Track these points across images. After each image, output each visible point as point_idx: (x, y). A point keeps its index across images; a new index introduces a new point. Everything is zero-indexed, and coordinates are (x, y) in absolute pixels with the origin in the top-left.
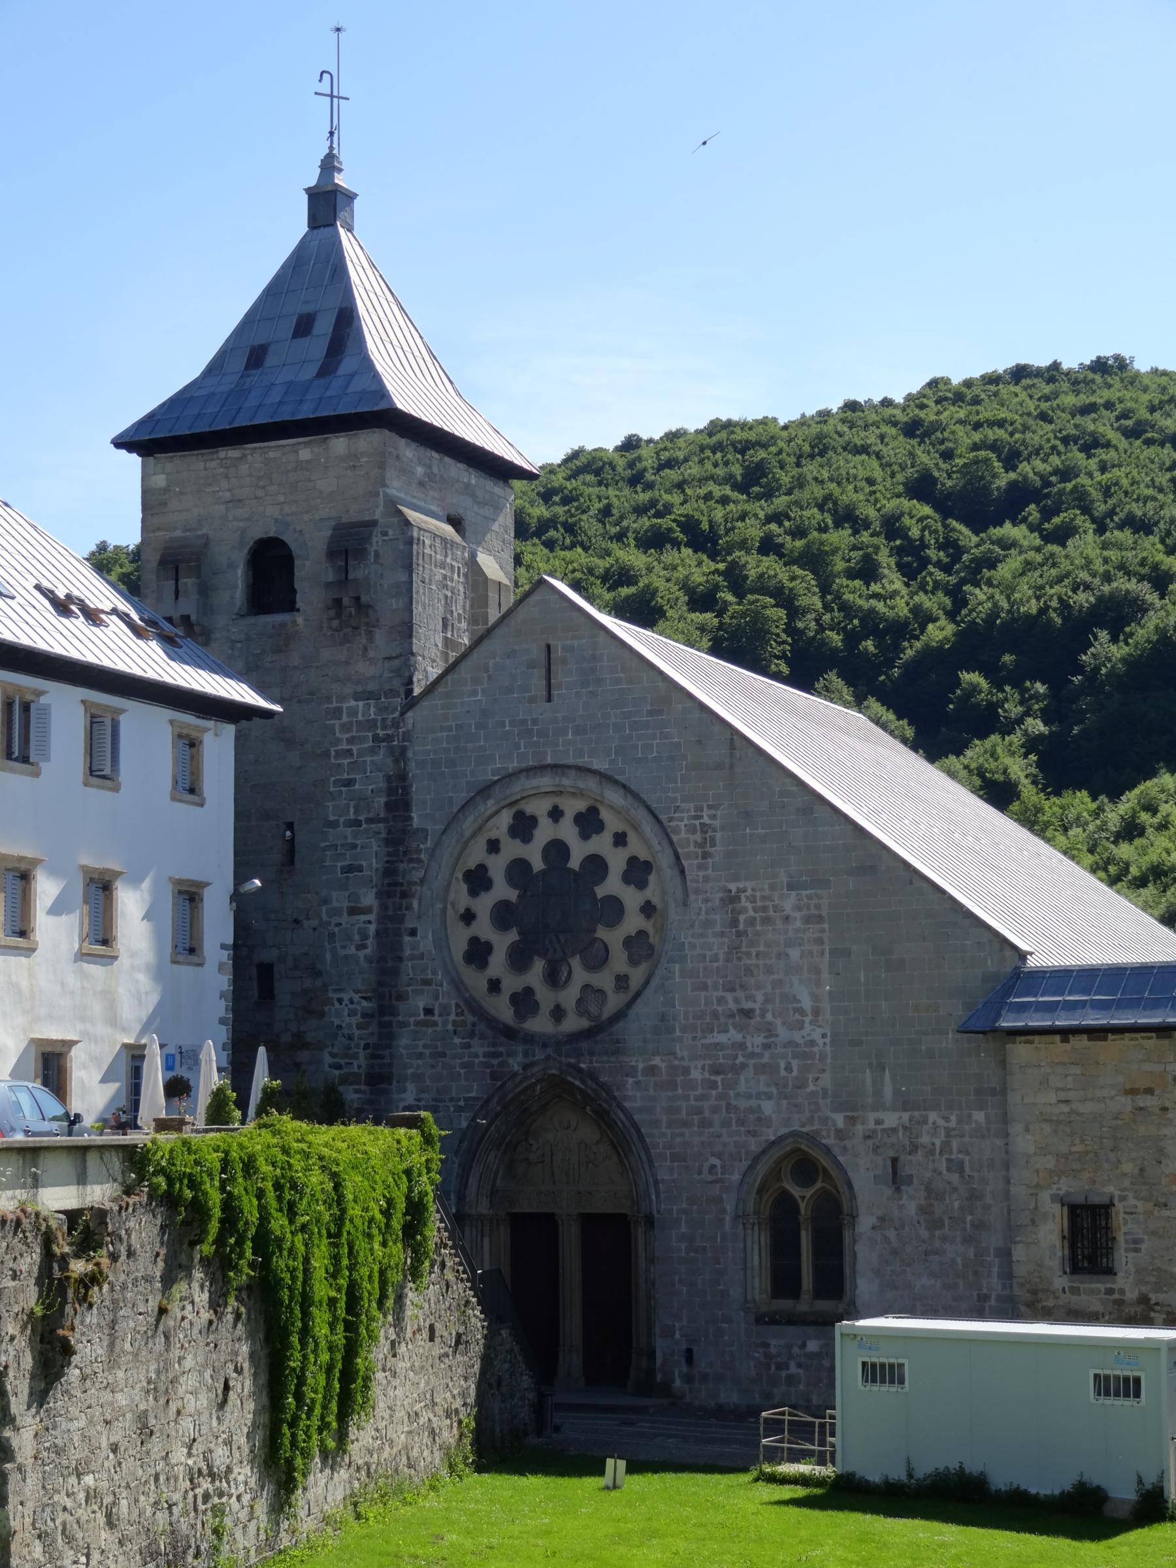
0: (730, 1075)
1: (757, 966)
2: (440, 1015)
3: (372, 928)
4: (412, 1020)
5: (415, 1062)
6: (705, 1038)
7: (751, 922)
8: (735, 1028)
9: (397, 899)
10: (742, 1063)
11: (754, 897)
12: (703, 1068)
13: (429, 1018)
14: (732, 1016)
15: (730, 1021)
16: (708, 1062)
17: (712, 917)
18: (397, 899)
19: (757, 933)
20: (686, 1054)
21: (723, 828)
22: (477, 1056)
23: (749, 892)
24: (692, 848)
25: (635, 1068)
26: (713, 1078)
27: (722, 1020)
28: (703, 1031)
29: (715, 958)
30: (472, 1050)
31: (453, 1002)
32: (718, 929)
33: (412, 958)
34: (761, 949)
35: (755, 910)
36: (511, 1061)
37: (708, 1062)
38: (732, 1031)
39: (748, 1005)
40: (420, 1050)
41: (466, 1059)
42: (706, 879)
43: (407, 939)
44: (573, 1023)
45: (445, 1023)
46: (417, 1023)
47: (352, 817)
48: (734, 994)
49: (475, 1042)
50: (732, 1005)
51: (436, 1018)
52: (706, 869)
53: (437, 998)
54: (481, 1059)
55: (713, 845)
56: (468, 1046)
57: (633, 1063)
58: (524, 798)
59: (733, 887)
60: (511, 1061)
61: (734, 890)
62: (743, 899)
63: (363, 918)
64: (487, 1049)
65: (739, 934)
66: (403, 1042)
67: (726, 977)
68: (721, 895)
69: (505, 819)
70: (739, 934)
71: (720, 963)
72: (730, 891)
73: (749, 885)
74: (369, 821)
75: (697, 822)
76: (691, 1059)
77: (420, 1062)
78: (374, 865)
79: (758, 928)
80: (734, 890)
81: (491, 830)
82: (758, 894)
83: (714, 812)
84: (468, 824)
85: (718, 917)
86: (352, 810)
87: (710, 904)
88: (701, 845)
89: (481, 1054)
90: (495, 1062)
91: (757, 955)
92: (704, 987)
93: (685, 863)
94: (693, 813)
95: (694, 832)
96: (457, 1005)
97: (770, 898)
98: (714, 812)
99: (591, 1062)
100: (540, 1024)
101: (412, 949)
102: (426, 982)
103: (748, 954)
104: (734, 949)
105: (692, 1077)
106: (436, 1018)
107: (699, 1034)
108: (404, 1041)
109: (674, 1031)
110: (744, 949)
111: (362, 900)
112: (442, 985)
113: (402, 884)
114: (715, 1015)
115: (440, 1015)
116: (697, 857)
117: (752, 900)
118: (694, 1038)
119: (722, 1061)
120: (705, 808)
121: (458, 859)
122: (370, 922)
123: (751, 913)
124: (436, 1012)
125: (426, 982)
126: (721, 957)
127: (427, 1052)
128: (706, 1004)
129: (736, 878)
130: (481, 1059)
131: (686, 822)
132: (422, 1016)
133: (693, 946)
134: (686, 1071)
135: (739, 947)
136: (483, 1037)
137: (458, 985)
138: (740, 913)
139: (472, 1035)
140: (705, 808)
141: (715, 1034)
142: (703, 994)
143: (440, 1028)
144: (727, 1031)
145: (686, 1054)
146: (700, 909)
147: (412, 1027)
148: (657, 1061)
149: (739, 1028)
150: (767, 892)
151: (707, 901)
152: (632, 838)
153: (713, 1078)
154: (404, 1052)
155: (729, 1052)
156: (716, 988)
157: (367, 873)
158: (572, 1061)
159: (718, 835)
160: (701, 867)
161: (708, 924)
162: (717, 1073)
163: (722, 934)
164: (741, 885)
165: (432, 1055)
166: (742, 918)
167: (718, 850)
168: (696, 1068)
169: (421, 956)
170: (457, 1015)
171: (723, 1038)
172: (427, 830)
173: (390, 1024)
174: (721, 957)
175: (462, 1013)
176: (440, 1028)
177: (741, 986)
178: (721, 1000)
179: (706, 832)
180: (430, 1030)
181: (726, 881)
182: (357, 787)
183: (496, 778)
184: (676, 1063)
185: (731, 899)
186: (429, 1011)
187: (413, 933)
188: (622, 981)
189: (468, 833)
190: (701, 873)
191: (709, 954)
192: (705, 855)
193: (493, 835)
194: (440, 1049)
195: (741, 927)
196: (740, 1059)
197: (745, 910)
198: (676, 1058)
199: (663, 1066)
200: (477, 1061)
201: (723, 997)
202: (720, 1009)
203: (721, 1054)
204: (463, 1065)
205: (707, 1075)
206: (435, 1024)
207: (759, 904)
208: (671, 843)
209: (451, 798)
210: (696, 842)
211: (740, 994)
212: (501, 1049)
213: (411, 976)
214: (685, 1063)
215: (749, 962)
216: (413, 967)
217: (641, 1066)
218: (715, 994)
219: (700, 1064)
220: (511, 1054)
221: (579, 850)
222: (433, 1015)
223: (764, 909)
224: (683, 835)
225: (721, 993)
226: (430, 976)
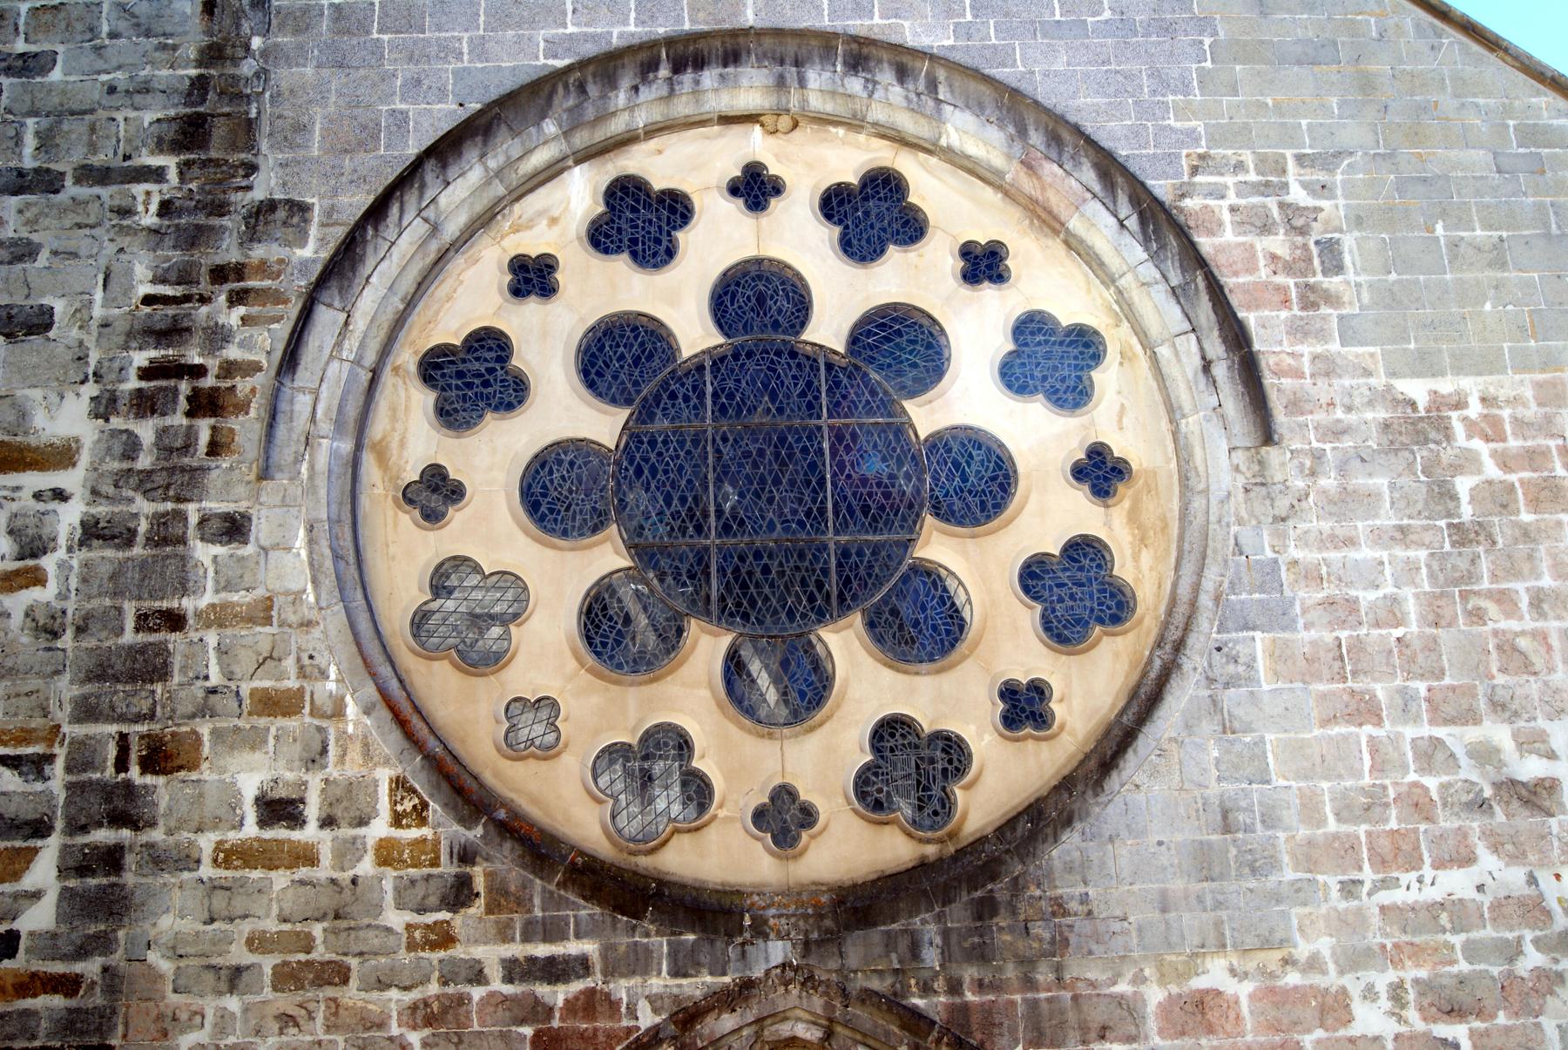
0: (1502, 1019)
1: (1541, 637)
2: (328, 822)
3: (69, 517)
4: (206, 843)
5: (210, 1005)
6: (1386, 884)
7: (1499, 498)
8: (1496, 849)
9: (178, 419)
10: (1539, 973)
11: (1496, 423)
12: (1397, 993)
13: (280, 833)
14: (1482, 805)
15: (1475, 825)
16: (1413, 972)
17: (1360, 481)
18: (178, 419)
19: (1526, 533)
20: (1324, 945)
21: (1358, 222)
22: (479, 977)
23: (1475, 410)
24: (1264, 273)
25: (1130, 1008)
26: (1444, 1030)
27: (1447, 822)
28: (1380, 862)
29: (1392, 613)
30: (459, 952)
31: (384, 776)
32: (1387, 519)
33: (218, 617)
34: (1547, 582)
35: (1505, 463)
36: (621, 988)
37: (1413, 972)
38: (1488, 861)
39: (1531, 769)
40: (239, 954)
41: (433, 988)
42: (1327, 367)
43: (204, 553)
44: (850, 847)
45: (348, 852)
46: (228, 856)
47: (29, 163)
48: (1472, 734)
49: (462, 921)
50: (1468, 771)
51: (310, 832)
52: (1322, 335)
53: (316, 757)
54: (497, 985)
55: (1334, 265)
56: (443, 938)
57: (1123, 987)
58: (652, 131)
59: (1417, 390)
60: (621, 988)
61: (1422, 402)
62: (1459, 429)
63: (33, 480)
64: (517, 950)
65: (1462, 536)
66: (171, 917)
67: (1441, 674)
68: (1382, 414)
69: (580, 194)
70: (1462, 536)
71: (1413, 627)
72: (1413, 405)
73: (1471, 385)
74: (92, 175)
75: (1272, 203)
76: (1354, 960)
77: (233, 1003)
78: (98, 312)
79: (1526, 517)
80: (1422, 402)
81: (530, 225)
82: (1506, 413)
83: (1322, 177)
84: (460, 192)
85: (1381, 482)
86: (30, 142)
87: (1348, 443)
88: (1297, 265)
89: (495, 973)
90: (559, 995)
91: (1538, 601)
92: (1367, 710)
93: (1250, 318)
94: (1252, 177)
95: (1266, 228)
96: (399, 784)
97: (1547, 426)
98: (1322, 177)
99: (954, 987)
100: (721, 854)
101: (226, 586)
102: (275, 704)
103: (1505, 600)
104: (1453, 590)
105: (1355, 1030)
106: (310, 832)
107: (1368, 875)
108: (167, 924)
109: (1274, 864)
110: (1485, 584)
111: (39, 420)
112: (338, 712)
113: (199, 371)
114: (1419, 805)
115: (328, 822)
116: (1286, 302)
117: (1491, 430)
118: (1350, 888)
119: (1463, 966)
120: (1291, 165)
121: (411, 303)
122: (60, 495)
123: (1492, 471)
124: (312, 811)
125: (275, 704)
126: (1412, 608)
127: (268, 963)
128: (1378, 768)
129: (1425, 365)
130: (497, 985)
131: (1232, 198)
132: (251, 829)
133: (1313, 576)
134: (1334, 1008)
135: (1471, 577)
136: (500, 898)
137: (406, 717)
138: (1457, 469)
139: (459, 894)
140: (1291, 165)
141: (1428, 872)
142: (1368, 729)
143: (324, 871)
144: (1468, 860)
145: (1324, 945)
146: (1318, 456)
147: (206, 871)
148: (1215, 974)
149: (1508, 847)
150: (1532, 412)
151: (1336, 432)
152: (1028, 254)
153: (1444, 1030)
154: (166, 966)
155: (1488, 932)
156: (1406, 707)
157: (64, 331)
158: (875, 984)
159: (1348, 242)
160: (1299, 331)
161: (1346, 502)
162: (1454, 1012)
163: (1403, 534)
164: (1446, 386)
165: (286, 978)
166: (1463, 485)
167: (1351, 283)
168: (1370, 994)
169: (263, 612)
170: (397, 820)
171: (1457, 883)
172: (302, 209)
173: (112, 858)
174: (1412, 608)
175: (420, 815)
176: (324, 871)
177: (1499, 706)
178: (1431, 754)
179: (1303, 231)
180: (281, 879)
181: (1393, 374)
182: (56, 75)
183: (560, 63)
184: (1293, 978)
185: (1419, 429)
186: (279, 809)
187: (234, 528)
188: (1024, 707)
189: (452, 229)
190: (1306, 349)
191: (1366, 597)
192: (1312, 298)
193: (533, 244)
194: (320, 953)
195: (1467, 512)
196: (1532, 959)
197: (1467, 463)
198: (1287, 962)
199: (1243, 991)
200: (477, 993)
201: (1437, 743)
202: (1432, 783)
203: (1457, 940)
204: (423, 1015)
205: (1412, 1014)
206: (307, 856)
207: (1513, 443)
208: (1195, 260)
209: (400, 119)
210: (1274, 257)
211: (1500, 734)
212: (573, 947)
213: (215, 679)
214: (1331, 979)
215: (1513, 625)
216: (222, 651)
217: (1155, 995)
218: (1409, 732)
219: (1383, 980)
220: (639, 963)
221: (839, 298)
222: (297, 821)
223: (1534, 458)
224: (1229, 236)
225: (1426, 730)
226: (292, 683)
